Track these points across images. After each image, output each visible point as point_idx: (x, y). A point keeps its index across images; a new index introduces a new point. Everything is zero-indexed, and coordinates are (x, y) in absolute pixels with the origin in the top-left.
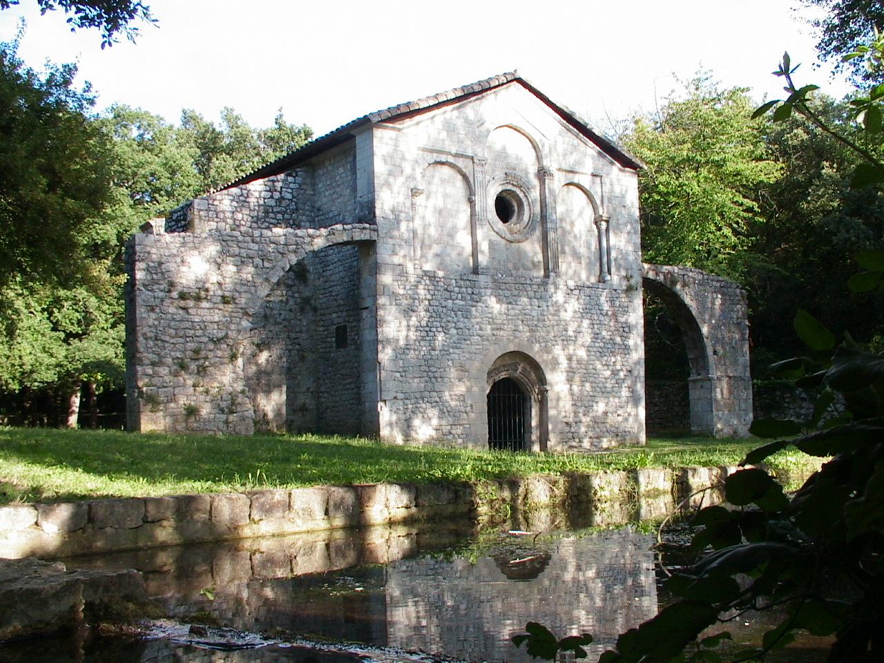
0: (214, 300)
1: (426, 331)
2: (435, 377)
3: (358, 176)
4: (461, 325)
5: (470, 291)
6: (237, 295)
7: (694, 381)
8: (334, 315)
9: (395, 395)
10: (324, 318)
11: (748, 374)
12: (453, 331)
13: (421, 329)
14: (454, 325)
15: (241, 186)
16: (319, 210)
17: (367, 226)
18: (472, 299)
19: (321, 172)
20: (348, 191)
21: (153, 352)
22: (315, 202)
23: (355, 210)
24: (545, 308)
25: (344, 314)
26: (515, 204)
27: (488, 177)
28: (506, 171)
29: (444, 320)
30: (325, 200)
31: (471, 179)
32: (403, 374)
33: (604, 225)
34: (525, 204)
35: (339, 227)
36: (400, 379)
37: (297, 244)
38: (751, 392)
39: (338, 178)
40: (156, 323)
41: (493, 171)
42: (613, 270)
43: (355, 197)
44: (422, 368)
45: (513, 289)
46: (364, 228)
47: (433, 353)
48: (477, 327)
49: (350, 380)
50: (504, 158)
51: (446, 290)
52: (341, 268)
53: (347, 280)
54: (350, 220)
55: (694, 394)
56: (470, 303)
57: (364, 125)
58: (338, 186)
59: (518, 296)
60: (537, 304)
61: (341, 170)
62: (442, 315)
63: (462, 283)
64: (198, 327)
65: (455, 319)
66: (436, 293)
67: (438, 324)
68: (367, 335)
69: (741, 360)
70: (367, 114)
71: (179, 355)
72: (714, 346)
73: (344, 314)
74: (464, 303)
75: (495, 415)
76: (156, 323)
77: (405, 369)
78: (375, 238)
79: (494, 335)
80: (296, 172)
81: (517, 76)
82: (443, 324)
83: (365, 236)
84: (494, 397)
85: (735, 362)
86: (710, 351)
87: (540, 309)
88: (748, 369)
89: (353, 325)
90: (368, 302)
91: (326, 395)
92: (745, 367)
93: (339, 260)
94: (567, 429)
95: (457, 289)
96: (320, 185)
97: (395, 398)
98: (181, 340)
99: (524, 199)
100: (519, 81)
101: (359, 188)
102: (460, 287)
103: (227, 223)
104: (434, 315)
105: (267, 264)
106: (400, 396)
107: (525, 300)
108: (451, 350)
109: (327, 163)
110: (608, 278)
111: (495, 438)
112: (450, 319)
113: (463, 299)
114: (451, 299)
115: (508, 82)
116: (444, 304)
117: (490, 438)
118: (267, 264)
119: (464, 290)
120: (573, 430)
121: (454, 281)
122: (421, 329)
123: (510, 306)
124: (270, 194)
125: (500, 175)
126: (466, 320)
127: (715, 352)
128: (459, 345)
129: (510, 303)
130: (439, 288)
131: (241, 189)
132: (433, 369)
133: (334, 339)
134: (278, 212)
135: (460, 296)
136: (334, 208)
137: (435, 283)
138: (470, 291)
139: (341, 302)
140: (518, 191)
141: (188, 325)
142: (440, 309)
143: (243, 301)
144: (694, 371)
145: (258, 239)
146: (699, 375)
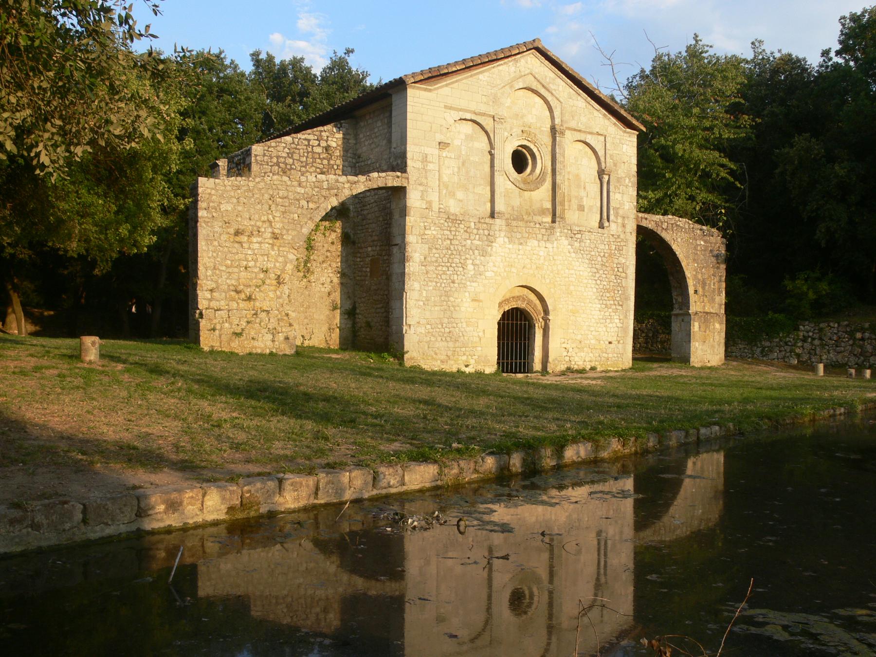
3: (393, 130)
4: (478, 262)
6: (284, 232)
7: (677, 315)
8: (370, 249)
9: (418, 320)
10: (361, 251)
11: (723, 311)
12: (470, 267)
14: (471, 261)
15: (293, 135)
16: (359, 157)
17: (399, 174)
18: (488, 240)
19: (362, 124)
20: (385, 142)
21: (212, 280)
22: (357, 150)
23: (390, 158)
24: (551, 249)
25: (378, 248)
26: (529, 158)
27: (506, 134)
28: (523, 128)
29: (463, 258)
30: (364, 149)
31: (492, 136)
33: (606, 178)
34: (538, 157)
35: (375, 175)
37: (338, 188)
38: (724, 326)
39: (376, 130)
40: (215, 254)
41: (511, 129)
42: (612, 217)
43: (390, 148)
44: (442, 298)
46: (398, 177)
47: (452, 285)
49: (381, 305)
50: (522, 117)
51: (466, 231)
52: (376, 209)
53: (381, 219)
54: (385, 168)
55: (675, 326)
56: (486, 243)
57: (399, 86)
58: (376, 137)
59: (528, 238)
61: (379, 124)
62: (462, 253)
64: (250, 259)
65: (473, 257)
68: (396, 268)
69: (717, 299)
70: (402, 75)
71: (233, 282)
72: (695, 285)
73: (378, 248)
75: (503, 339)
76: (215, 254)
78: (405, 185)
80: (341, 124)
81: (536, 45)
82: (462, 261)
83: (396, 183)
84: (504, 324)
85: (712, 300)
86: (691, 291)
88: (723, 307)
89: (385, 258)
90: (397, 240)
91: (360, 316)
92: (721, 305)
93: (375, 202)
94: (565, 354)
95: (475, 231)
96: (361, 136)
98: (236, 270)
99: (537, 154)
100: (538, 49)
101: (393, 140)
102: (478, 229)
103: (279, 167)
105: (311, 205)
106: (423, 321)
107: (536, 243)
108: (468, 283)
109: (367, 117)
110: (606, 224)
111: (503, 359)
112: (468, 256)
114: (469, 239)
115: (528, 50)
117: (498, 359)
118: (311, 205)
119: (481, 231)
120: (569, 354)
121: (472, 224)
123: (521, 247)
124: (317, 142)
125: (517, 131)
126: (482, 258)
127: (696, 292)
129: (521, 244)
131: (293, 138)
133: (368, 270)
134: (324, 158)
136: (371, 156)
138: (486, 232)
139: (376, 238)
140: (532, 146)
141: (241, 256)
142: (460, 248)
143: (290, 237)
144: (676, 306)
145: (304, 184)
146: (681, 309)
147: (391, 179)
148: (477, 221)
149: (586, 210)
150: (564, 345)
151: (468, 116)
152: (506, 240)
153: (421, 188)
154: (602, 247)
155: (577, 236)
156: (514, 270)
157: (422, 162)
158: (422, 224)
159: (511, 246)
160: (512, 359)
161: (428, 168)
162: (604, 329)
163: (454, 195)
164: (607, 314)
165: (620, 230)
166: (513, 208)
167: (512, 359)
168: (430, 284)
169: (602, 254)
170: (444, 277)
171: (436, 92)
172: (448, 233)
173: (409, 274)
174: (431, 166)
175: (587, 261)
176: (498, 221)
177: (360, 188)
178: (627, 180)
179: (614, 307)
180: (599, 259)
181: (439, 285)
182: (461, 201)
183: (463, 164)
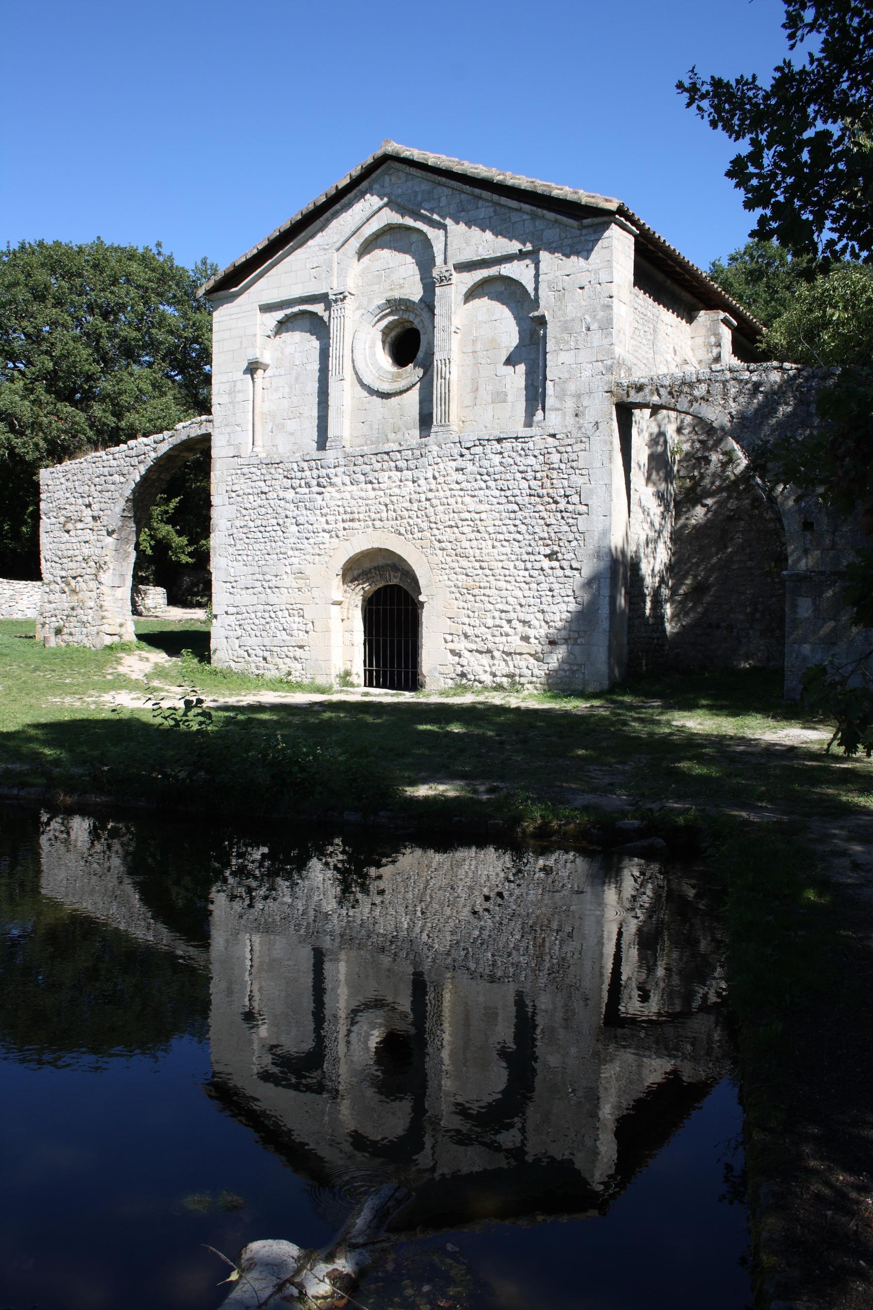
0: (86, 521)
1: (261, 532)
2: (269, 588)
4: (301, 520)
5: (315, 473)
12: (294, 529)
13: (255, 530)
18: (319, 485)
32: (234, 584)
36: (232, 590)
41: (370, 301)
45: (374, 461)
48: (323, 520)
56: (316, 489)
60: (410, 478)
63: (305, 465)
66: (274, 482)
67: (274, 522)
74: (307, 490)
77: (236, 579)
78: (210, 430)
79: (345, 529)
82: (281, 522)
83: (195, 432)
87: (416, 484)
95: (299, 475)
97: (226, 613)
104: (270, 511)
106: (232, 610)
107: (396, 475)
108: (290, 553)
113: (308, 485)
116: (282, 494)
121: (295, 466)
122: (255, 530)
123: (369, 486)
128: (299, 546)
130: (277, 476)
132: (268, 577)
135: (303, 482)
137: (273, 471)
138: (315, 473)
147: (188, 428)
148: (299, 459)
149: (510, 398)
150: (450, 646)
151: (296, 309)
152: (347, 480)
153: (228, 430)
154: (531, 460)
155: (473, 451)
156: (356, 525)
157: (230, 394)
158: (229, 479)
159: (354, 487)
160: (399, 666)
161: (237, 400)
162: (540, 616)
163: (283, 426)
164: (545, 586)
165: (570, 420)
166: (371, 426)
167: (399, 666)
168: (239, 558)
169: (530, 475)
170: (256, 546)
171: (248, 291)
172: (262, 484)
173: (215, 548)
174: (240, 397)
175: (497, 493)
176: (330, 456)
177: (164, 448)
178: (589, 319)
179: (560, 573)
180: (524, 484)
181: (250, 558)
182: (292, 434)
183: (297, 379)
